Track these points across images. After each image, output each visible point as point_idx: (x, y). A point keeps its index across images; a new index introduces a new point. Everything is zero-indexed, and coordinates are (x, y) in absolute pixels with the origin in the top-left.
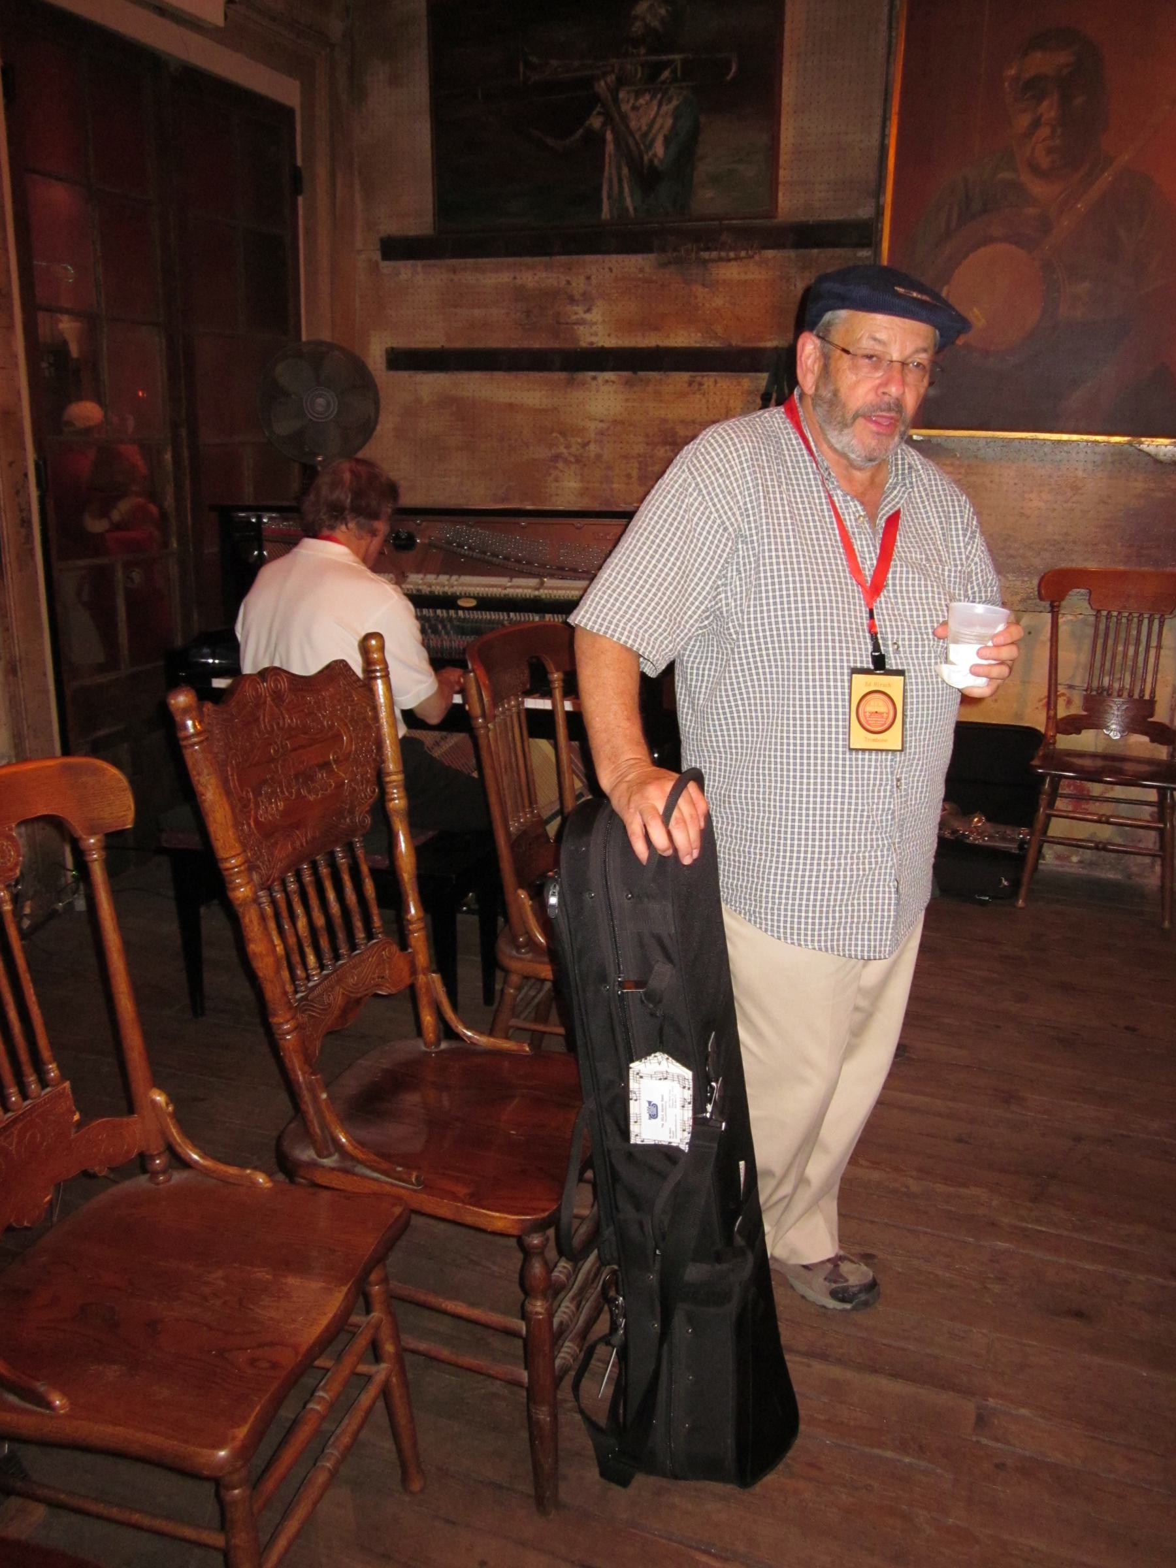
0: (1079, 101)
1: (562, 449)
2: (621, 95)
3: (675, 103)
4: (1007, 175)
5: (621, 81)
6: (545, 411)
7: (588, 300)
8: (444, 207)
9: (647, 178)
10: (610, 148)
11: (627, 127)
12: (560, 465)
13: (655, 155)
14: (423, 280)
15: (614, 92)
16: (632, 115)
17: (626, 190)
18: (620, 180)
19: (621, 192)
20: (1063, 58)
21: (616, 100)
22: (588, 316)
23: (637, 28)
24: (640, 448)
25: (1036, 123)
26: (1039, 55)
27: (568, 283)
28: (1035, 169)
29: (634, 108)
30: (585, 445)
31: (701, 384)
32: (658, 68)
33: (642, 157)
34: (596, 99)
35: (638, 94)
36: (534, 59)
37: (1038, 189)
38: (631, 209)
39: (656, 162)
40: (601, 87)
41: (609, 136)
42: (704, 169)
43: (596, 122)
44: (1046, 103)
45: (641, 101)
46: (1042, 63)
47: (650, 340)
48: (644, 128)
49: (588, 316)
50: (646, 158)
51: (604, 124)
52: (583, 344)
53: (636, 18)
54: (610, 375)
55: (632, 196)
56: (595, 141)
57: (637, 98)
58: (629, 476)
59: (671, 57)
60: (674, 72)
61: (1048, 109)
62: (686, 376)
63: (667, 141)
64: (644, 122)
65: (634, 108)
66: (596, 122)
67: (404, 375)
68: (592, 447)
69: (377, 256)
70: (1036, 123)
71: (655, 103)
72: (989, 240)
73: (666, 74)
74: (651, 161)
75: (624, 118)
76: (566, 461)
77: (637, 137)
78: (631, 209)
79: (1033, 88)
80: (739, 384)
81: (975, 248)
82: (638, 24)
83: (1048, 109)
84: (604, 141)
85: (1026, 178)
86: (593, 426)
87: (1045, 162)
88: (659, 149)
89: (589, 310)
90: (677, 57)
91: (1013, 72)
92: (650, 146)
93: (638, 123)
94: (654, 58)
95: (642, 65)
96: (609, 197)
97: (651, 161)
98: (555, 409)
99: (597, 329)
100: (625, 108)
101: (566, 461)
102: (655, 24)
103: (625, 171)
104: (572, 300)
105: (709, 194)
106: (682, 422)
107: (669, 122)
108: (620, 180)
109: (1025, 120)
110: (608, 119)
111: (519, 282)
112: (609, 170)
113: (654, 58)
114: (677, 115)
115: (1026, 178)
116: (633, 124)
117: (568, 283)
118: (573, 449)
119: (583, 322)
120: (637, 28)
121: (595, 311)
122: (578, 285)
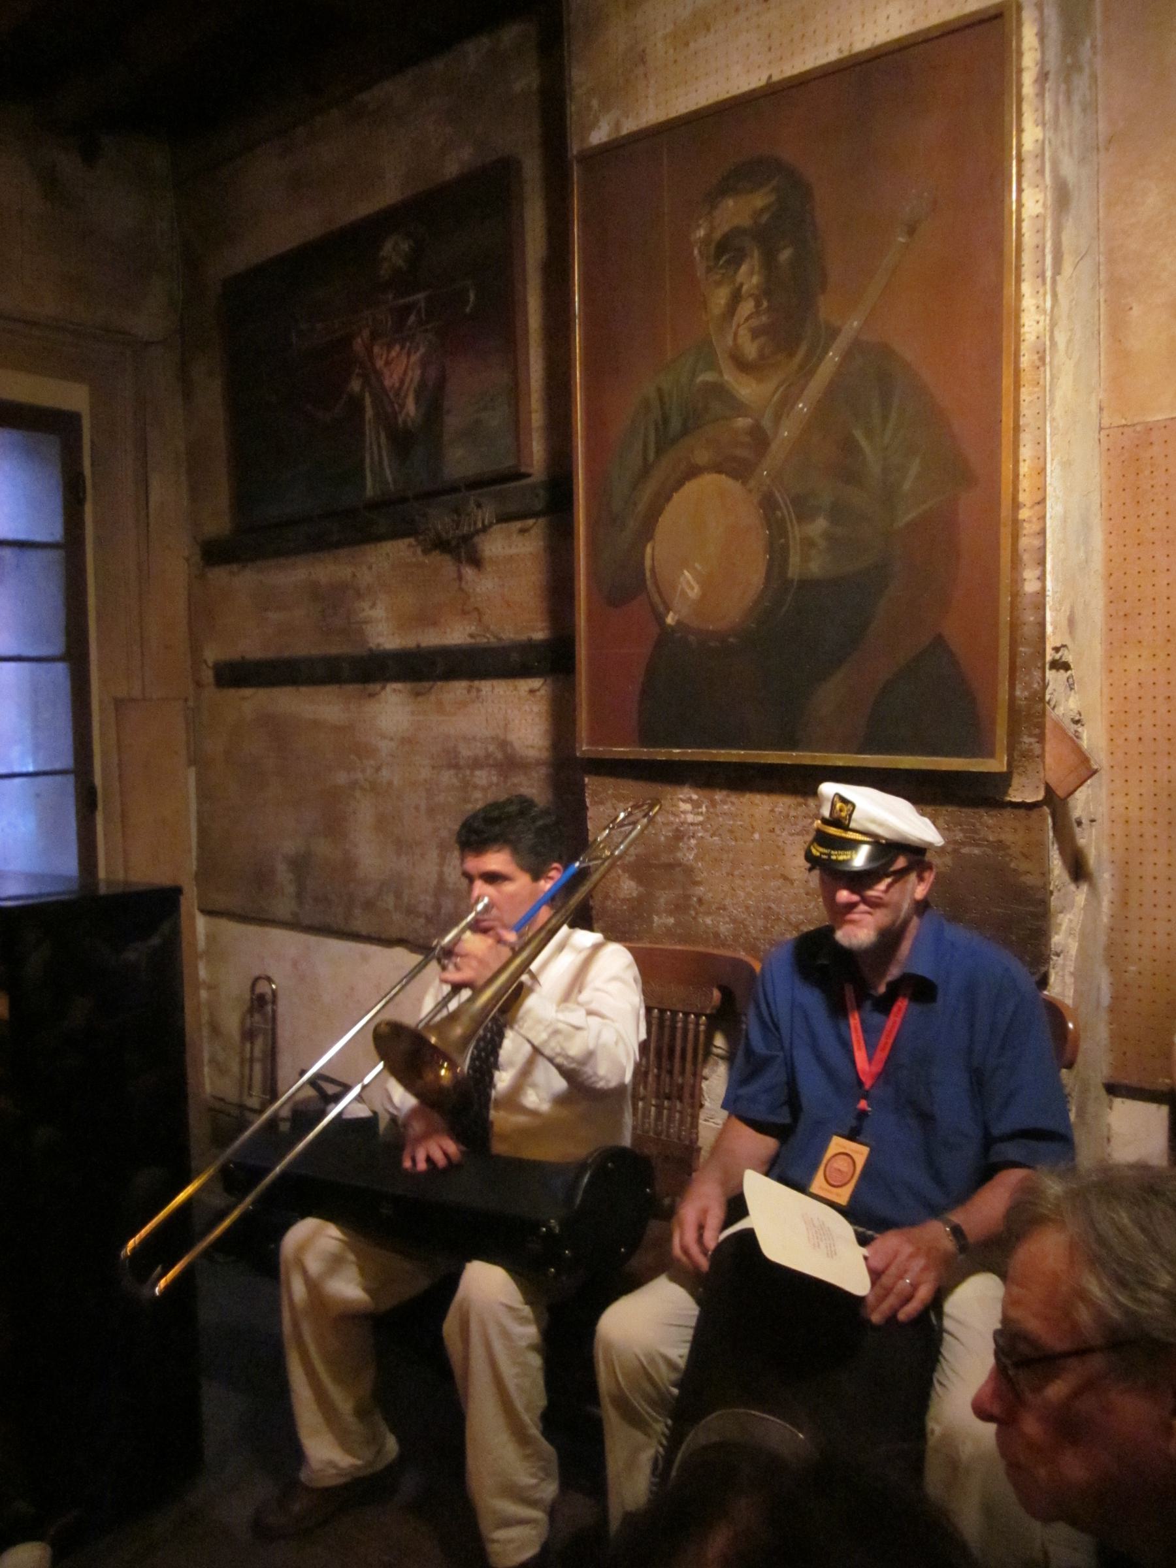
0: (785, 255)
1: (360, 776)
2: (376, 349)
3: (422, 350)
4: (708, 377)
5: (374, 336)
8: (242, 501)
9: (402, 441)
10: (369, 413)
11: (382, 383)
12: (358, 794)
13: (408, 414)
14: (241, 582)
15: (369, 350)
16: (386, 372)
20: (760, 200)
21: (371, 357)
23: (385, 271)
24: (425, 773)
25: (736, 298)
26: (731, 203)
28: (743, 365)
30: (378, 769)
31: (479, 690)
33: (396, 418)
35: (390, 347)
37: (747, 389)
38: (390, 479)
39: (410, 424)
42: (453, 422)
44: (744, 268)
45: (393, 354)
46: (737, 211)
48: (397, 385)
50: (400, 420)
51: (362, 390)
54: (398, 686)
55: (390, 466)
57: (389, 352)
58: (417, 808)
59: (411, 299)
61: (749, 276)
64: (396, 377)
65: (387, 363)
66: (355, 385)
67: (232, 692)
68: (385, 772)
70: (736, 298)
72: (693, 472)
74: (405, 422)
75: (379, 374)
76: (362, 789)
77: (392, 396)
78: (390, 479)
79: (727, 250)
80: (516, 688)
81: (679, 484)
82: (386, 265)
83: (749, 276)
85: (730, 377)
87: (751, 350)
88: (411, 407)
89: (373, 606)
90: (420, 296)
91: (702, 233)
94: (401, 301)
96: (371, 471)
97: (405, 422)
101: (362, 789)
102: (400, 263)
103: (383, 439)
105: (459, 453)
106: (464, 738)
107: (418, 372)
109: (720, 298)
110: (366, 382)
113: (401, 301)
114: (424, 364)
115: (730, 377)
116: (387, 383)
117: (354, 575)
118: (369, 771)
120: (385, 271)
121: (379, 605)
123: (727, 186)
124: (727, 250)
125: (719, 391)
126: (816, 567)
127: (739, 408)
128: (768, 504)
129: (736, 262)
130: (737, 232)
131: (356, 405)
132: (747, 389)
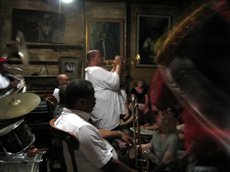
5: (42, 24)
6: (34, 70)
7: (41, 55)
17: (42, 38)
18: (41, 36)
21: (41, 26)
22: (41, 57)
27: (38, 52)
29: (44, 27)
32: (48, 23)
34: (38, 25)
35: (45, 26)
36: (29, 19)
39: (47, 35)
40: (39, 24)
41: (40, 30)
43: (38, 28)
47: (51, 60)
49: (41, 57)
52: (40, 61)
53: (45, 16)
56: (38, 31)
62: (56, 65)
63: (49, 32)
64: (45, 29)
69: (6, 47)
71: (47, 27)
73: (49, 24)
88: (47, 33)
92: (46, 32)
98: (36, 70)
99: (42, 59)
100: (43, 27)
102: (47, 17)
103: (42, 35)
104: (39, 55)
106: (56, 72)
108: (41, 36)
110: (40, 28)
111: (30, 52)
112: (40, 34)
114: (50, 29)
116: (44, 29)
119: (40, 58)
122: (40, 52)
131: (38, 30)
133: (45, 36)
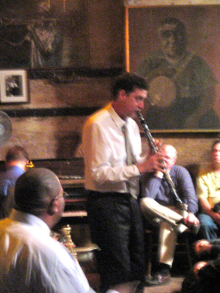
9: (46, 55)
11: (39, 40)
17: (40, 60)
19: (38, 59)
20: (174, 26)
21: (35, 32)
28: (169, 56)
34: (27, 31)
37: (170, 61)
39: (50, 51)
40: (29, 28)
41: (33, 43)
43: (28, 38)
46: (168, 27)
50: (46, 49)
56: (27, 44)
58: (44, 151)
60: (54, 24)
61: (171, 40)
63: (53, 45)
64: (44, 39)
68: (30, 142)
70: (168, 43)
72: (158, 75)
73: (51, 25)
74: (48, 50)
75: (38, 38)
78: (41, 64)
79: (166, 34)
84: (30, 43)
86: (28, 135)
87: (171, 53)
88: (50, 47)
90: (54, 20)
91: (161, 29)
93: (41, 38)
95: (44, 22)
100: (38, 34)
103: (39, 53)
107: (53, 39)
109: (164, 43)
110: (32, 37)
112: (33, 52)
114: (55, 37)
123: (166, 21)
124: (166, 34)
125: (163, 60)
126: (187, 96)
127: (169, 64)
128: (176, 83)
129: (168, 36)
130: (168, 31)
132: (170, 61)
133: (46, 55)
